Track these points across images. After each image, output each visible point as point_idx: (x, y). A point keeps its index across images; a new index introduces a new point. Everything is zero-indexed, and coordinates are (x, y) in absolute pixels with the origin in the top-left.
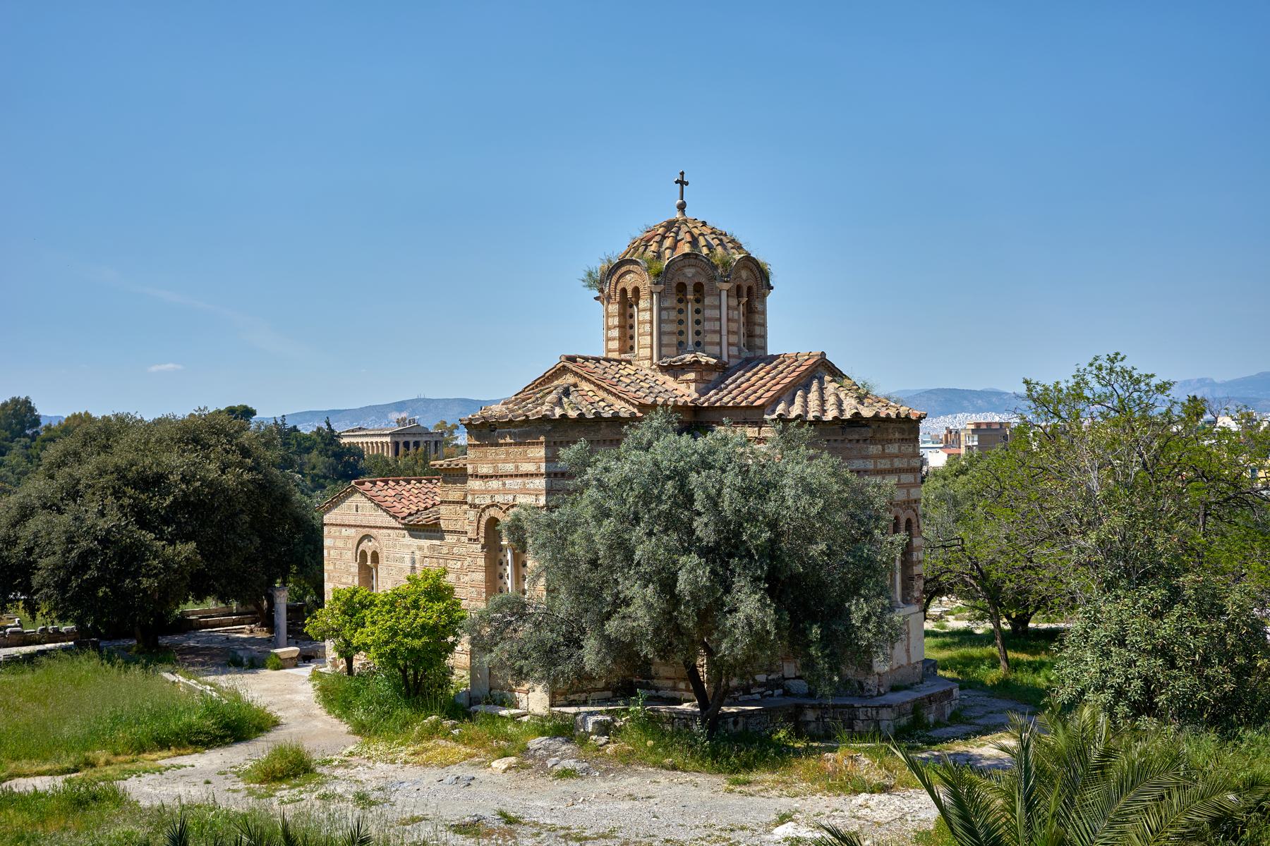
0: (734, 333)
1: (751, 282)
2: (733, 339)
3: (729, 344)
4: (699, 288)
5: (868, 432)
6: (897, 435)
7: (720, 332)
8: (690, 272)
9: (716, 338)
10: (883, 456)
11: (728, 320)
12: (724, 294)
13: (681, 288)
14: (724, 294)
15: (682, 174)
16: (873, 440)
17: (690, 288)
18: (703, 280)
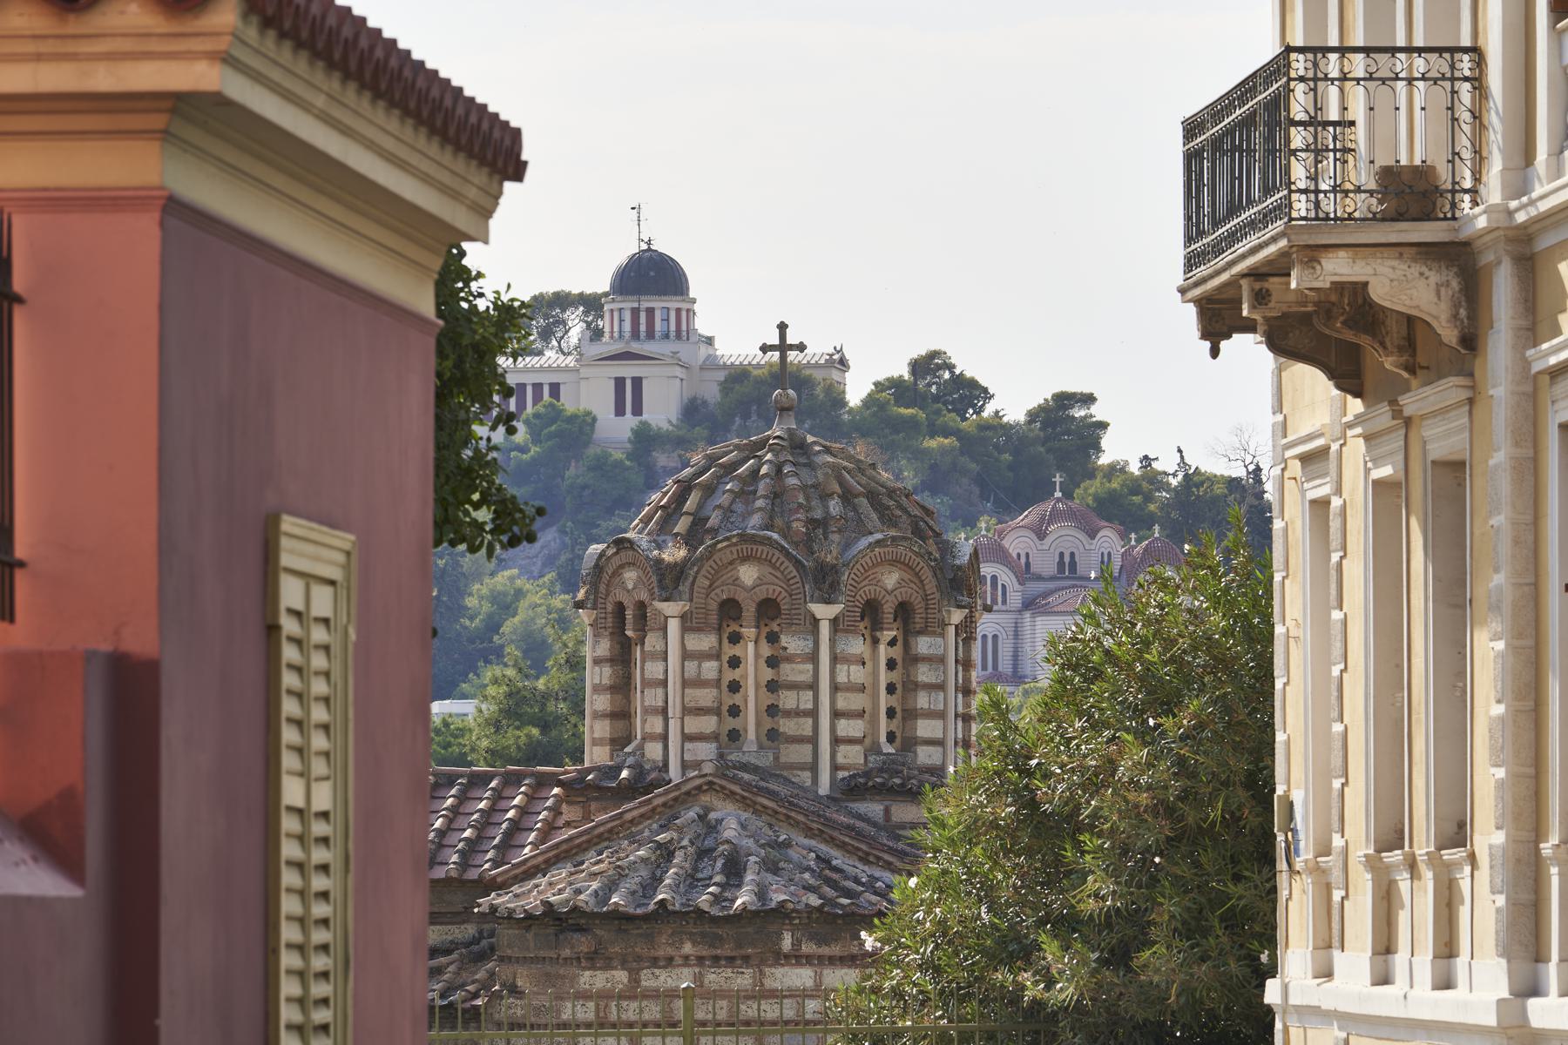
0: (700, 711)
1: (774, 590)
2: (694, 725)
3: (687, 738)
4: (641, 606)
5: (583, 943)
6: (688, 948)
7: (664, 711)
8: (630, 576)
9: (656, 725)
10: (633, 992)
11: (685, 683)
12: (674, 626)
13: (620, 608)
14: (674, 626)
15: (782, 327)
16: (596, 959)
17: (629, 614)
18: (644, 596)
